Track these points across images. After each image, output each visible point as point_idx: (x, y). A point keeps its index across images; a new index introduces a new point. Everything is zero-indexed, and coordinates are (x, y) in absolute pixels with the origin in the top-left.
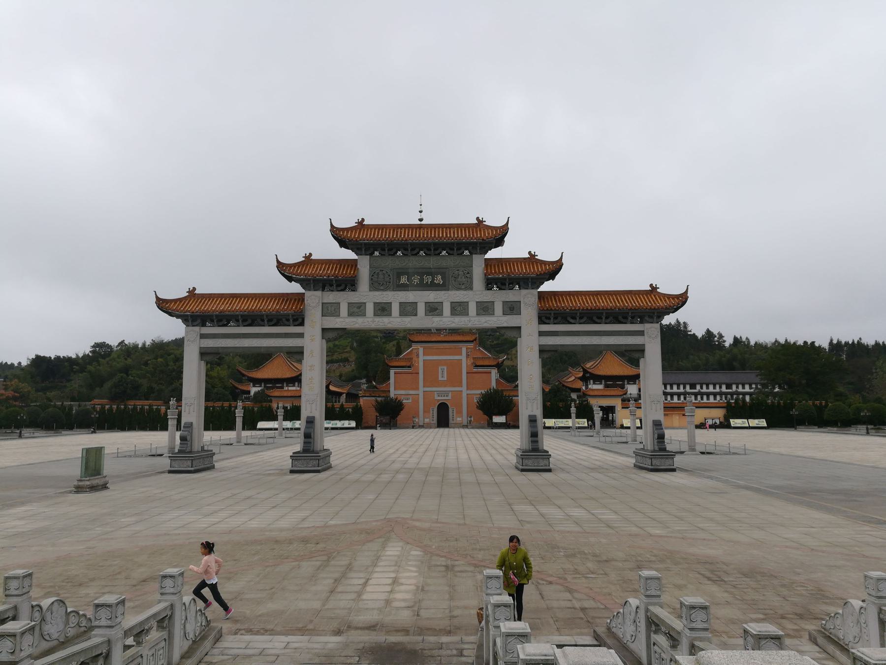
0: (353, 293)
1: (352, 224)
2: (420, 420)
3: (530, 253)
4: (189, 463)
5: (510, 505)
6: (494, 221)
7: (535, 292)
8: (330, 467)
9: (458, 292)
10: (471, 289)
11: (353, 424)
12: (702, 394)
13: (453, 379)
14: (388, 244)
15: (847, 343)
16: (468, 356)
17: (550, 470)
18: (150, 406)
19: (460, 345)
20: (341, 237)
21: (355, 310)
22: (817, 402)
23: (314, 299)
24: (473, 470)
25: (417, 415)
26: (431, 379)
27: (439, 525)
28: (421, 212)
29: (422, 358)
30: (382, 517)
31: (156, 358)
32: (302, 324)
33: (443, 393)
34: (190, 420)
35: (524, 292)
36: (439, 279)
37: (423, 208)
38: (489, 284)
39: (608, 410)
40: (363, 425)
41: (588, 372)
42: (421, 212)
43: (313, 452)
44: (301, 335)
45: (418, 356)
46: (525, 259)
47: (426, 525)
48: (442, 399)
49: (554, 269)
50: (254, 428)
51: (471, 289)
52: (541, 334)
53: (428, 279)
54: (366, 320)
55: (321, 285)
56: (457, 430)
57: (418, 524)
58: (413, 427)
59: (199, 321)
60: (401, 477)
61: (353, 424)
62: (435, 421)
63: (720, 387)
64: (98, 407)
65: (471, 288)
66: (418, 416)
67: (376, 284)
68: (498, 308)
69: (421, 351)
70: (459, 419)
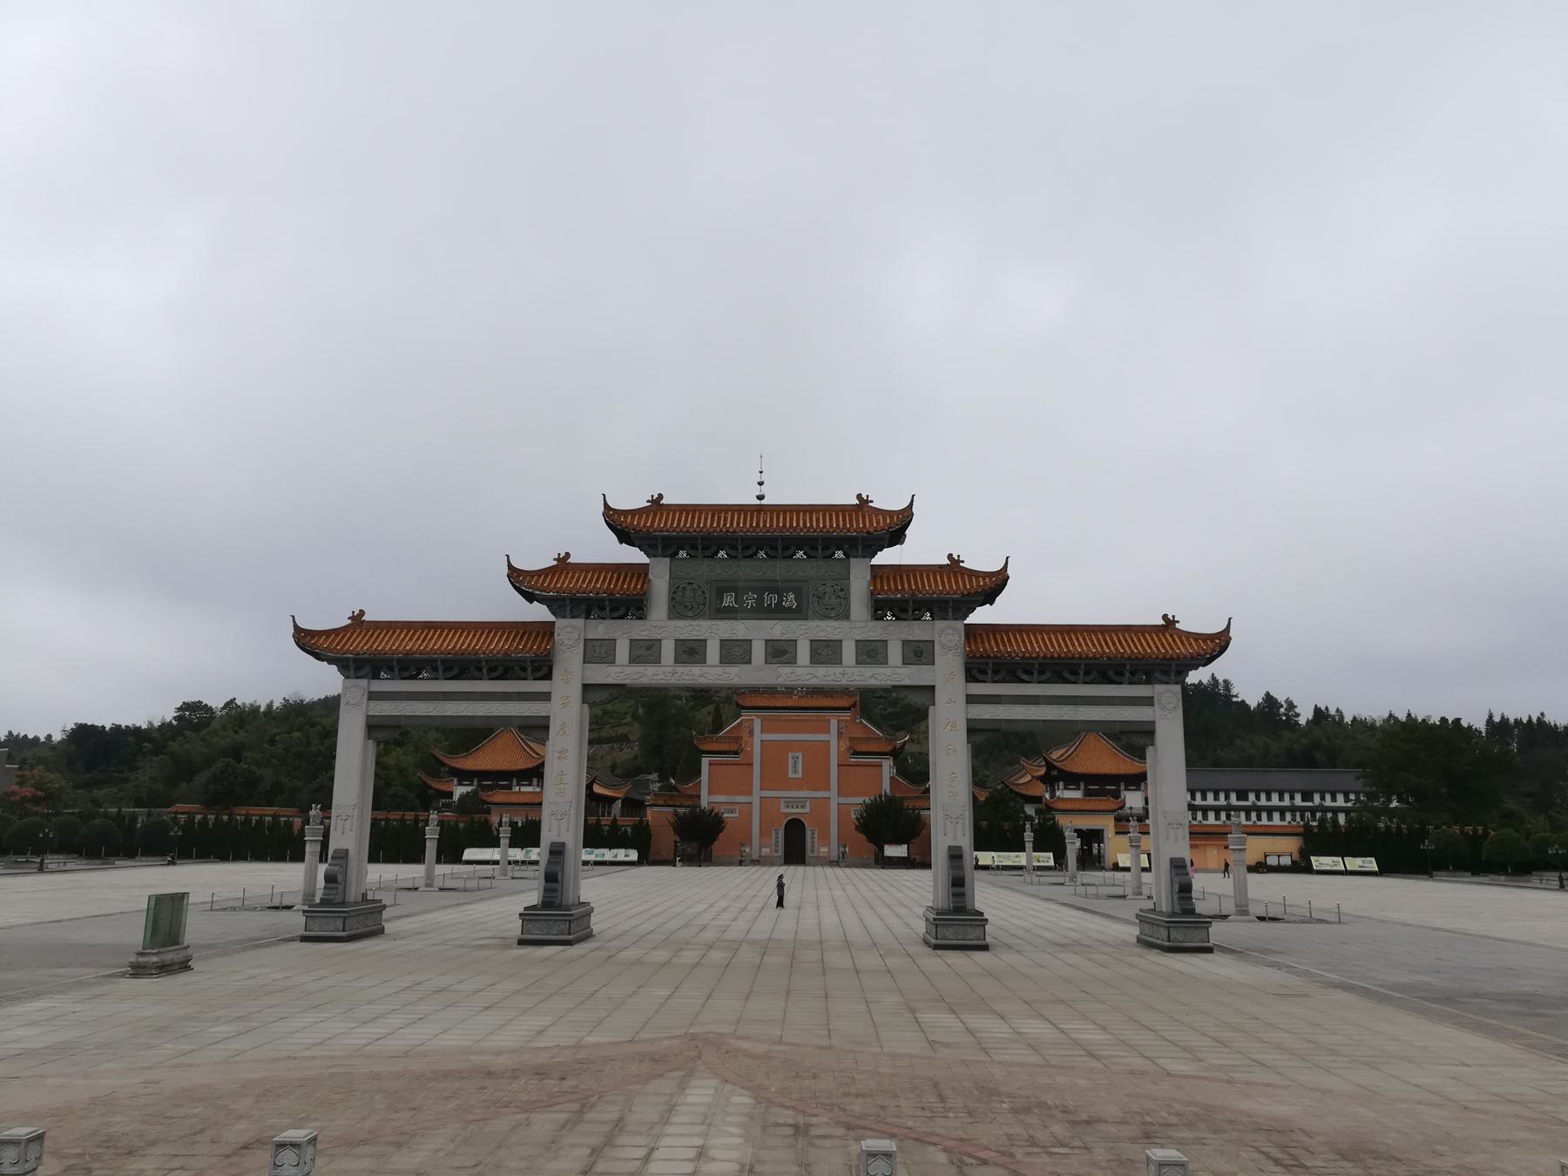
0: (639, 622)
1: (641, 502)
2: (754, 850)
3: (950, 556)
4: (339, 924)
5: (913, 1011)
6: (887, 500)
7: (959, 625)
8: (589, 936)
9: (824, 624)
10: (847, 617)
11: (633, 855)
12: (1259, 810)
13: (816, 777)
14: (703, 539)
15: (1518, 722)
16: (840, 734)
17: (985, 948)
18: (275, 817)
19: (827, 714)
20: (621, 524)
21: (643, 651)
22: (1469, 829)
23: (571, 633)
24: (847, 945)
25: (748, 840)
26: (775, 776)
27: (783, 1048)
28: (761, 484)
29: (758, 737)
30: (682, 1032)
31: (289, 732)
32: (548, 676)
33: (796, 801)
34: (344, 846)
35: (940, 624)
36: (790, 600)
37: (764, 478)
38: (879, 608)
39: (1091, 837)
40: (651, 858)
41: (1055, 768)
42: (761, 484)
43: (560, 907)
44: (546, 697)
45: (751, 733)
46: (941, 566)
47: (760, 1048)
49: (993, 586)
50: (456, 859)
51: (847, 617)
52: (971, 699)
53: (771, 599)
54: (660, 670)
55: (583, 607)
56: (819, 870)
57: (745, 1045)
58: (741, 863)
59: (367, 670)
60: (717, 956)
61: (633, 855)
62: (781, 852)
63: (1292, 798)
64: (182, 818)
65: (845, 615)
66: (749, 842)
67: (678, 609)
68: (895, 652)
70: (824, 850)
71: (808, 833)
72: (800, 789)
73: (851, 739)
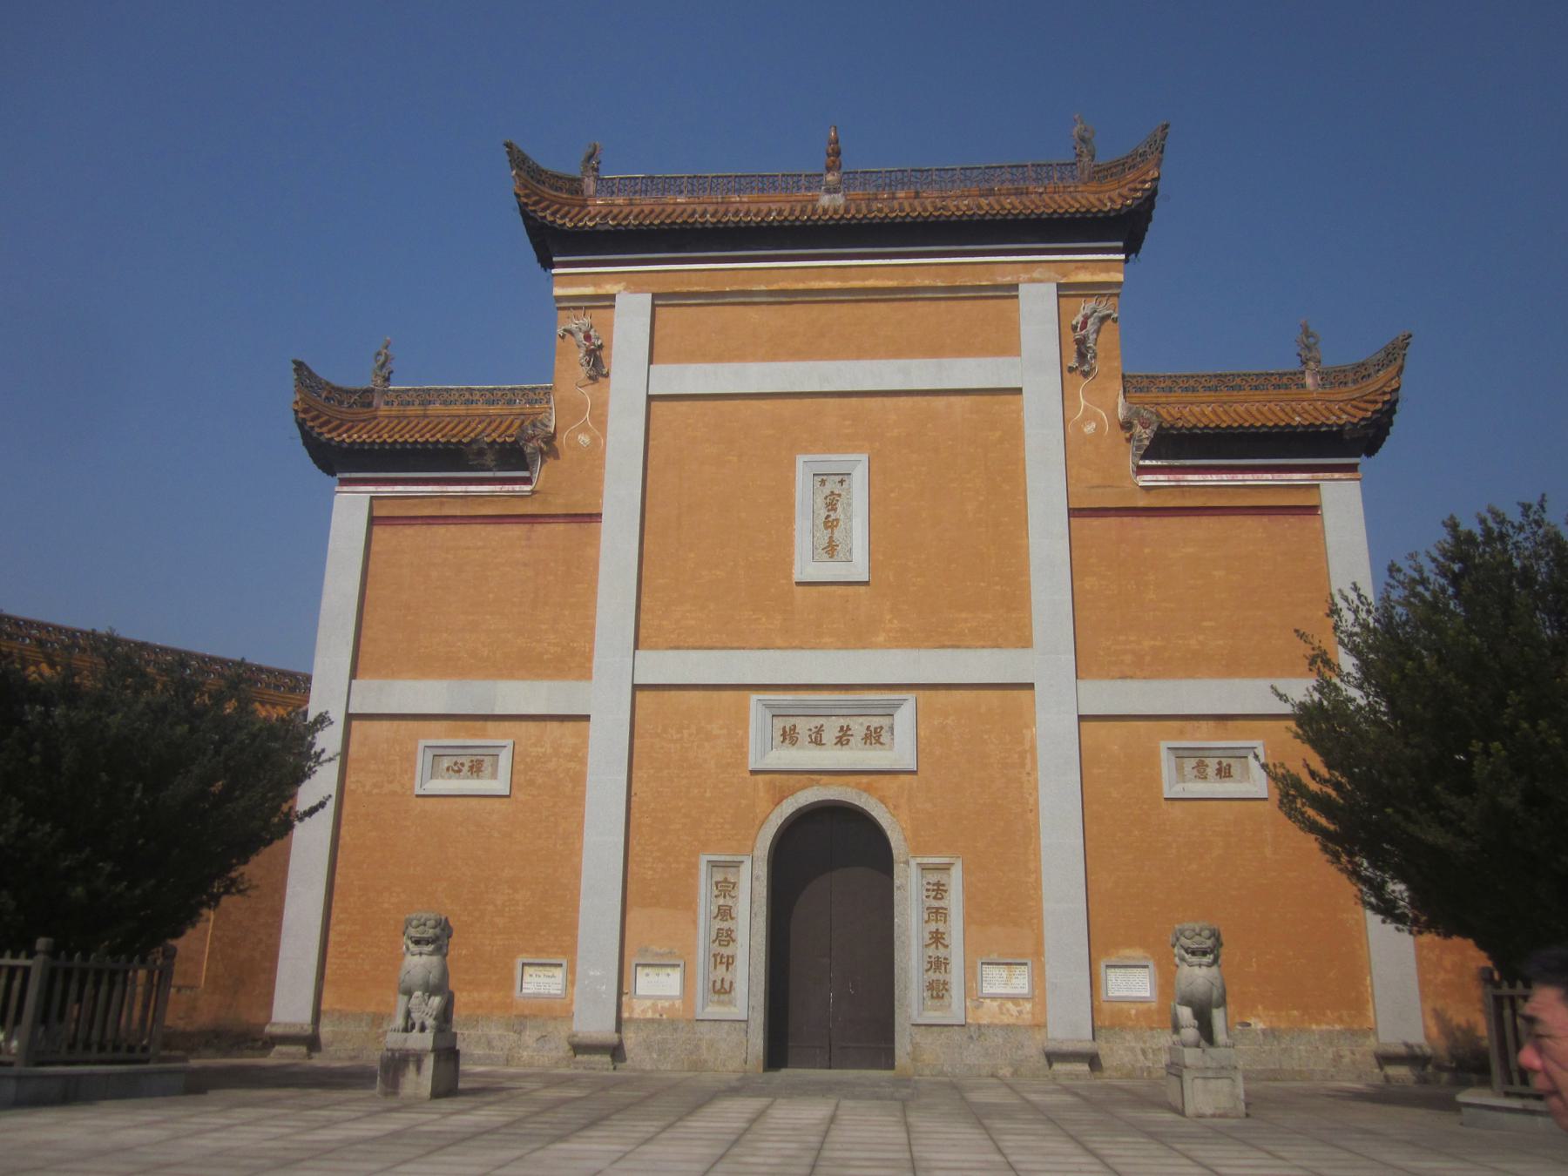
13: (948, 572)
16: (1079, 357)
26: (716, 567)
48: (826, 763)
66: (554, 934)
71: (909, 883)
72: (858, 637)
73: (1130, 384)
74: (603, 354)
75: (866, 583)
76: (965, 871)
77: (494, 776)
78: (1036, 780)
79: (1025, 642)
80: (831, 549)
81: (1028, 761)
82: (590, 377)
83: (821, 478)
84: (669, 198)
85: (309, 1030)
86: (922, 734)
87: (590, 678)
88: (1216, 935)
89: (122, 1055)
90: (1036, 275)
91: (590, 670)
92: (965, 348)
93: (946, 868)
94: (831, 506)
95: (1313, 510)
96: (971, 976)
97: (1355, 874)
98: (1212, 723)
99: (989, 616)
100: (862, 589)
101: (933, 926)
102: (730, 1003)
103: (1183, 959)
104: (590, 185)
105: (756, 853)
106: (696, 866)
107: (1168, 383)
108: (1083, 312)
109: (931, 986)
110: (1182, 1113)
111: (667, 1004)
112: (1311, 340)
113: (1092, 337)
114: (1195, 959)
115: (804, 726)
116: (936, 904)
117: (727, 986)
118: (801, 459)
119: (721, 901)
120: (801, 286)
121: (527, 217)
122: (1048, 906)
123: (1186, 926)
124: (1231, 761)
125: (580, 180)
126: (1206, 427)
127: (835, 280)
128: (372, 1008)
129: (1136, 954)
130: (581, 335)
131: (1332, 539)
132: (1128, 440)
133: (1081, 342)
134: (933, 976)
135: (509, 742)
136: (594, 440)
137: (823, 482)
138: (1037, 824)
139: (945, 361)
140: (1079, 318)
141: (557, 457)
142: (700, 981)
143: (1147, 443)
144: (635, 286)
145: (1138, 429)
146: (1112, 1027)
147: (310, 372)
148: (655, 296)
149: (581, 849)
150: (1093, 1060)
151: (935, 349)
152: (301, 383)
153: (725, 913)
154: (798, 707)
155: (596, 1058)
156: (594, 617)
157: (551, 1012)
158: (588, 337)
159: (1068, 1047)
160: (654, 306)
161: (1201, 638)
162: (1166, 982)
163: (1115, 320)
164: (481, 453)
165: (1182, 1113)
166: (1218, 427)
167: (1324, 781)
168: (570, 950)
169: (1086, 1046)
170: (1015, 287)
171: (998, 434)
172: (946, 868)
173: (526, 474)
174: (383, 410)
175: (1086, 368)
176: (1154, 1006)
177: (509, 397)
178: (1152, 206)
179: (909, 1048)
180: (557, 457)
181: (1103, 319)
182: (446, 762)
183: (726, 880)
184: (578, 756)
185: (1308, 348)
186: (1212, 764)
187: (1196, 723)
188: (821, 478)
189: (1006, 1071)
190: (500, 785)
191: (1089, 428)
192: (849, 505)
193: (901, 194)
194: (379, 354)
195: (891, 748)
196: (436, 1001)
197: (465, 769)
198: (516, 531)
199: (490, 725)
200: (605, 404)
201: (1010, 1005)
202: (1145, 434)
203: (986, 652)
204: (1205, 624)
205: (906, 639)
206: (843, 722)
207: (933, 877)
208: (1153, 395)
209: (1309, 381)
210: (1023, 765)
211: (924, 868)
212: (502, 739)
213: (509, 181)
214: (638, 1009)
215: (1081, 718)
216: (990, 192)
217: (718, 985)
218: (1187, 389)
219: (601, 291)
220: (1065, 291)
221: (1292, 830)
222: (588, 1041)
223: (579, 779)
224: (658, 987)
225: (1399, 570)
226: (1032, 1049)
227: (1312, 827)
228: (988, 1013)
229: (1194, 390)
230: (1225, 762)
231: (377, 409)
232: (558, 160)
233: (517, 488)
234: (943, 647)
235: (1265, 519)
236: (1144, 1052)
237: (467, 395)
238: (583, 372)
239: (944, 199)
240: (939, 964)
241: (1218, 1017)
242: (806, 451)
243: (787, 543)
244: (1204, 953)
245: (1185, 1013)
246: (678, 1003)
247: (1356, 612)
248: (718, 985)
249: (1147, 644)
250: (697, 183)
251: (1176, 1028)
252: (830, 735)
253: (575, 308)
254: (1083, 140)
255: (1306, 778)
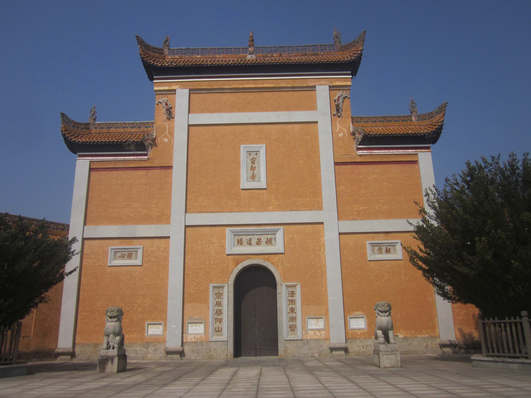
13: (293, 184)
16: (337, 111)
19: (308, 79)
29: (182, 118)
45: (170, 113)
48: (253, 251)
66: (159, 313)
69: (182, 97)
70: (315, 324)
71: (282, 292)
72: (263, 207)
74: (172, 110)
75: (266, 189)
76: (302, 287)
77: (136, 258)
78: (325, 255)
79: (320, 208)
80: (253, 177)
81: (322, 249)
82: (168, 118)
83: (249, 153)
84: (194, 56)
85: (71, 350)
86: (286, 240)
87: (170, 223)
88: (389, 306)
89: (3, 362)
90: (322, 83)
91: (170, 221)
92: (298, 107)
93: (295, 286)
94: (253, 162)
95: (416, 162)
96: (304, 323)
97: (434, 284)
98: (383, 234)
99: (308, 200)
100: (264, 191)
101: (291, 306)
102: (221, 335)
103: (378, 314)
104: (166, 51)
105: (229, 283)
106: (208, 288)
107: (367, 119)
108: (338, 95)
109: (290, 327)
110: (379, 367)
111: (199, 336)
112: (414, 105)
113: (341, 104)
114: (383, 314)
115: (245, 238)
116: (292, 298)
117: (220, 329)
118: (242, 146)
119: (217, 300)
120: (241, 86)
121: (144, 62)
122: (330, 298)
123: (379, 303)
124: (390, 247)
125: (163, 50)
126: (380, 134)
127: (253, 84)
128: (94, 342)
129: (360, 313)
130: (164, 104)
131: (422, 172)
132: (354, 139)
133: (337, 106)
134: (291, 323)
135: (141, 247)
136: (170, 140)
137: (250, 154)
138: (325, 270)
139: (292, 112)
140: (337, 97)
141: (156, 146)
142: (211, 328)
143: (360, 140)
144: (183, 87)
145: (357, 135)
146: (352, 338)
147: (67, 117)
148: (190, 90)
149: (168, 283)
150: (346, 350)
151: (288, 109)
152: (63, 121)
153: (219, 304)
154: (242, 232)
155: (175, 356)
156: (171, 202)
157: (158, 340)
158: (166, 104)
159: (337, 346)
160: (190, 93)
161: (379, 206)
162: (371, 322)
163: (349, 98)
164: (129, 145)
165: (379, 367)
166: (384, 134)
167: (423, 252)
168: (165, 319)
169: (344, 345)
170: (315, 87)
171: (310, 137)
172: (295, 286)
173: (145, 152)
174: (94, 131)
175: (339, 114)
176: (366, 331)
177: (139, 126)
178: (361, 59)
179: (283, 348)
180: (156, 146)
181: (345, 98)
182: (119, 254)
183: (219, 293)
184: (166, 251)
185: (413, 107)
186: (384, 249)
187: (378, 235)
188: (249, 153)
189: (316, 355)
190: (138, 262)
191: (341, 135)
192: (259, 162)
193: (275, 55)
194: (92, 111)
195: (275, 245)
196: (118, 338)
197: (126, 256)
198: (142, 172)
199: (135, 241)
200: (173, 128)
201: (317, 332)
202: (360, 137)
203: (307, 212)
204: (381, 201)
205: (280, 208)
206: (259, 237)
207: (290, 289)
208: (362, 124)
209: (413, 119)
210: (320, 250)
211: (288, 286)
212: (139, 246)
213: (137, 49)
214: (189, 338)
215: (340, 234)
216: (306, 54)
217: (217, 329)
218: (373, 122)
219: (171, 88)
220: (332, 88)
221: (415, 269)
222: (171, 350)
223: (166, 259)
224: (196, 330)
225: (449, 180)
226: (325, 348)
227: (420, 268)
228: (310, 335)
229: (375, 122)
230: (388, 248)
231: (91, 130)
232: (155, 42)
233: (142, 157)
234: (292, 210)
235: (400, 165)
236: (363, 346)
237: (124, 125)
238: (165, 117)
239: (290, 56)
240: (293, 319)
241: (391, 333)
242: (244, 144)
243: (237, 176)
244: (386, 312)
245: (380, 333)
246: (203, 336)
247: (434, 195)
248: (217, 329)
249: (361, 208)
250: (204, 51)
251: (377, 338)
252: (254, 242)
253: (162, 94)
254: (337, 37)
255: (418, 251)
